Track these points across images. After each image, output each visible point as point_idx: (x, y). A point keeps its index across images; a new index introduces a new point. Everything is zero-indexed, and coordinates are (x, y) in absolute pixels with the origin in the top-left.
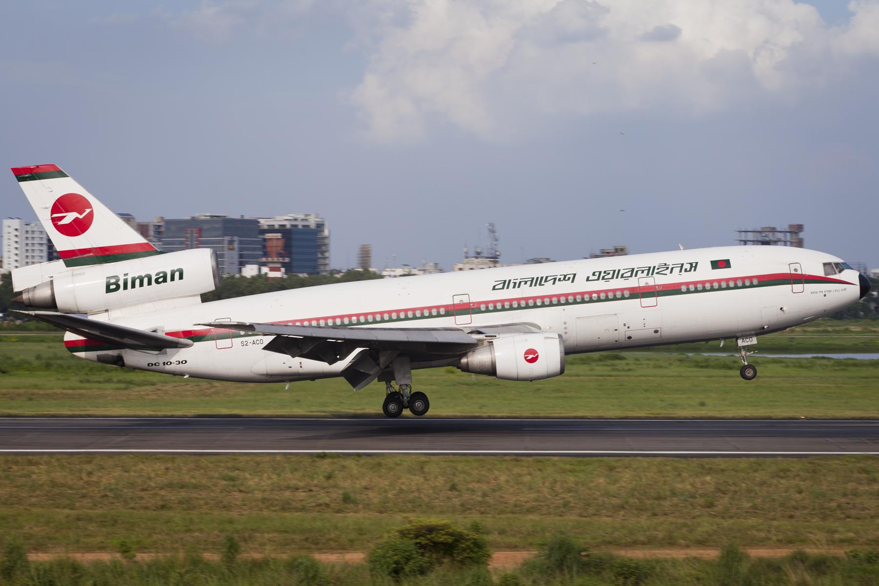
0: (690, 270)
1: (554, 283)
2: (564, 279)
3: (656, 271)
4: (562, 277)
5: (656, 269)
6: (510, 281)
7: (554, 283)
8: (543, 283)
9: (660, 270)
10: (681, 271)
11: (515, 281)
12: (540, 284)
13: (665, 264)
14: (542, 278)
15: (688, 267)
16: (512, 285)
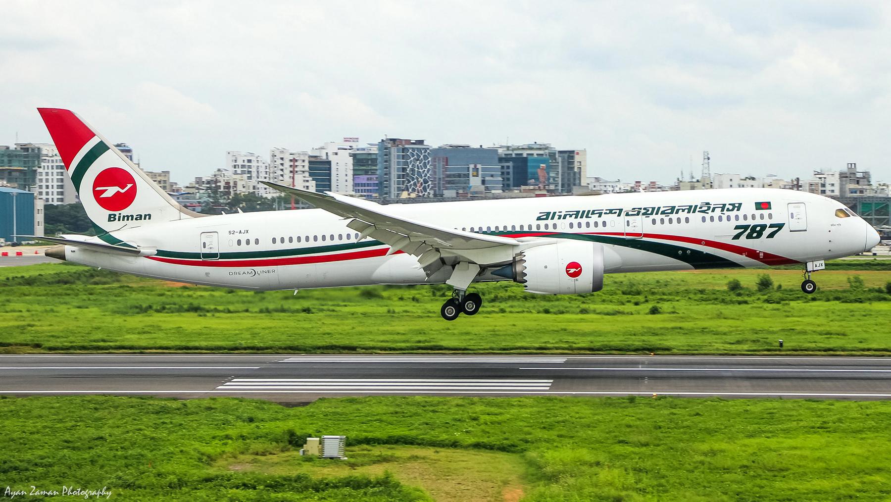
0: (733, 210)
1: (600, 216)
3: (698, 209)
4: (608, 212)
5: (698, 207)
6: (555, 213)
7: (600, 216)
8: (590, 215)
9: (704, 209)
10: (723, 210)
11: (560, 214)
12: (587, 217)
13: (708, 204)
14: (589, 211)
15: (731, 207)
16: (556, 217)
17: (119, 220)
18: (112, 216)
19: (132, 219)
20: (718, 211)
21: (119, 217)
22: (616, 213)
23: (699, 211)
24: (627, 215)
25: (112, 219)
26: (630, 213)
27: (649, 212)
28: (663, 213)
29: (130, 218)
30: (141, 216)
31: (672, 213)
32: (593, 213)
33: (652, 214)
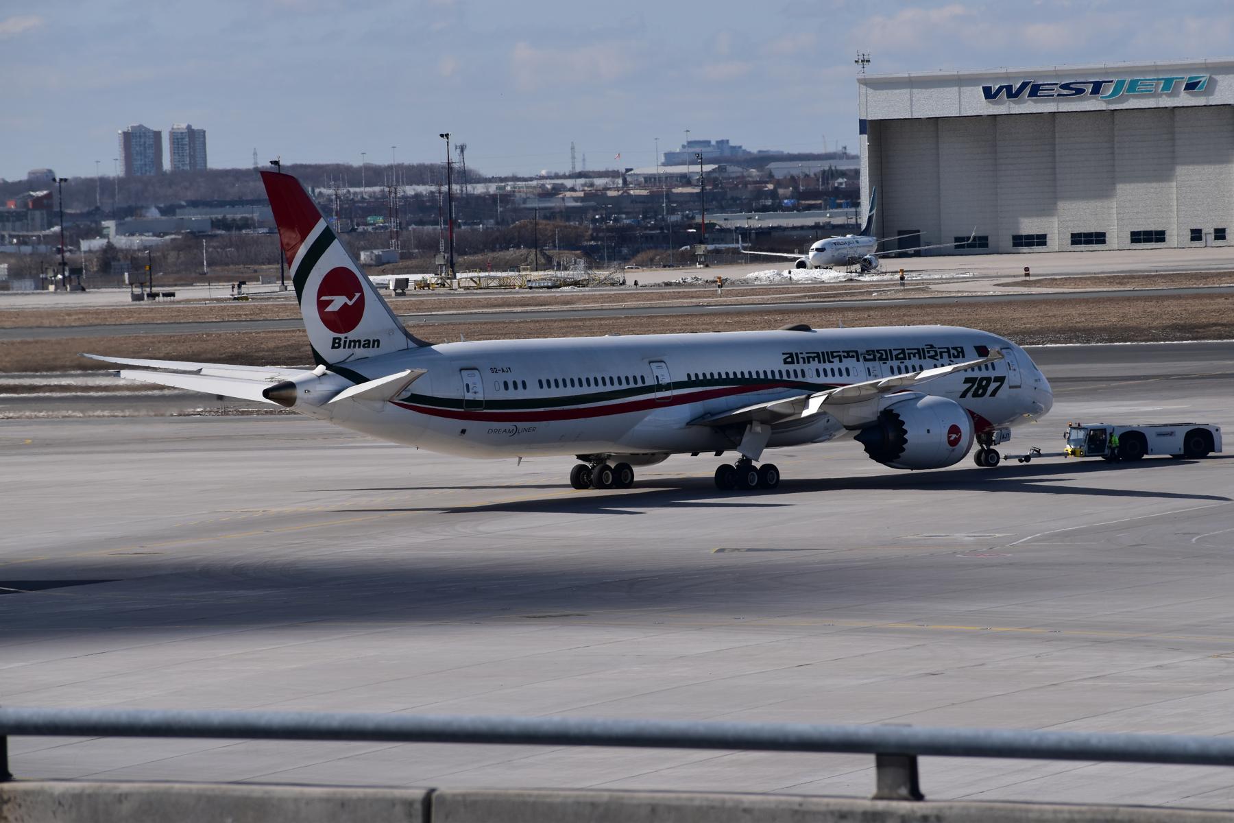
0: (958, 357)
2: (848, 356)
3: (927, 355)
7: (841, 361)
8: (831, 360)
9: (932, 353)
11: (802, 356)
16: (801, 360)
17: (344, 347)
18: (337, 341)
19: (359, 347)
20: (945, 355)
21: (345, 342)
22: (853, 357)
23: (929, 357)
24: (866, 360)
25: (336, 345)
26: (867, 357)
27: (884, 357)
28: (897, 359)
29: (357, 343)
30: (369, 341)
31: (904, 358)
32: (833, 357)
33: (887, 359)
